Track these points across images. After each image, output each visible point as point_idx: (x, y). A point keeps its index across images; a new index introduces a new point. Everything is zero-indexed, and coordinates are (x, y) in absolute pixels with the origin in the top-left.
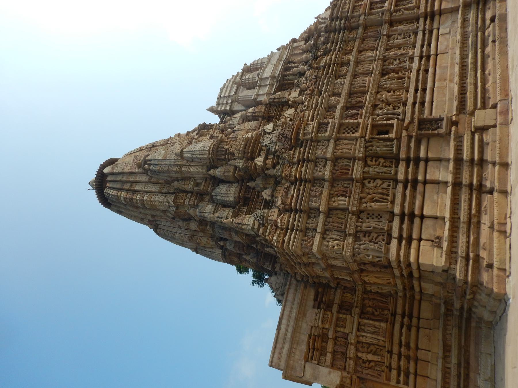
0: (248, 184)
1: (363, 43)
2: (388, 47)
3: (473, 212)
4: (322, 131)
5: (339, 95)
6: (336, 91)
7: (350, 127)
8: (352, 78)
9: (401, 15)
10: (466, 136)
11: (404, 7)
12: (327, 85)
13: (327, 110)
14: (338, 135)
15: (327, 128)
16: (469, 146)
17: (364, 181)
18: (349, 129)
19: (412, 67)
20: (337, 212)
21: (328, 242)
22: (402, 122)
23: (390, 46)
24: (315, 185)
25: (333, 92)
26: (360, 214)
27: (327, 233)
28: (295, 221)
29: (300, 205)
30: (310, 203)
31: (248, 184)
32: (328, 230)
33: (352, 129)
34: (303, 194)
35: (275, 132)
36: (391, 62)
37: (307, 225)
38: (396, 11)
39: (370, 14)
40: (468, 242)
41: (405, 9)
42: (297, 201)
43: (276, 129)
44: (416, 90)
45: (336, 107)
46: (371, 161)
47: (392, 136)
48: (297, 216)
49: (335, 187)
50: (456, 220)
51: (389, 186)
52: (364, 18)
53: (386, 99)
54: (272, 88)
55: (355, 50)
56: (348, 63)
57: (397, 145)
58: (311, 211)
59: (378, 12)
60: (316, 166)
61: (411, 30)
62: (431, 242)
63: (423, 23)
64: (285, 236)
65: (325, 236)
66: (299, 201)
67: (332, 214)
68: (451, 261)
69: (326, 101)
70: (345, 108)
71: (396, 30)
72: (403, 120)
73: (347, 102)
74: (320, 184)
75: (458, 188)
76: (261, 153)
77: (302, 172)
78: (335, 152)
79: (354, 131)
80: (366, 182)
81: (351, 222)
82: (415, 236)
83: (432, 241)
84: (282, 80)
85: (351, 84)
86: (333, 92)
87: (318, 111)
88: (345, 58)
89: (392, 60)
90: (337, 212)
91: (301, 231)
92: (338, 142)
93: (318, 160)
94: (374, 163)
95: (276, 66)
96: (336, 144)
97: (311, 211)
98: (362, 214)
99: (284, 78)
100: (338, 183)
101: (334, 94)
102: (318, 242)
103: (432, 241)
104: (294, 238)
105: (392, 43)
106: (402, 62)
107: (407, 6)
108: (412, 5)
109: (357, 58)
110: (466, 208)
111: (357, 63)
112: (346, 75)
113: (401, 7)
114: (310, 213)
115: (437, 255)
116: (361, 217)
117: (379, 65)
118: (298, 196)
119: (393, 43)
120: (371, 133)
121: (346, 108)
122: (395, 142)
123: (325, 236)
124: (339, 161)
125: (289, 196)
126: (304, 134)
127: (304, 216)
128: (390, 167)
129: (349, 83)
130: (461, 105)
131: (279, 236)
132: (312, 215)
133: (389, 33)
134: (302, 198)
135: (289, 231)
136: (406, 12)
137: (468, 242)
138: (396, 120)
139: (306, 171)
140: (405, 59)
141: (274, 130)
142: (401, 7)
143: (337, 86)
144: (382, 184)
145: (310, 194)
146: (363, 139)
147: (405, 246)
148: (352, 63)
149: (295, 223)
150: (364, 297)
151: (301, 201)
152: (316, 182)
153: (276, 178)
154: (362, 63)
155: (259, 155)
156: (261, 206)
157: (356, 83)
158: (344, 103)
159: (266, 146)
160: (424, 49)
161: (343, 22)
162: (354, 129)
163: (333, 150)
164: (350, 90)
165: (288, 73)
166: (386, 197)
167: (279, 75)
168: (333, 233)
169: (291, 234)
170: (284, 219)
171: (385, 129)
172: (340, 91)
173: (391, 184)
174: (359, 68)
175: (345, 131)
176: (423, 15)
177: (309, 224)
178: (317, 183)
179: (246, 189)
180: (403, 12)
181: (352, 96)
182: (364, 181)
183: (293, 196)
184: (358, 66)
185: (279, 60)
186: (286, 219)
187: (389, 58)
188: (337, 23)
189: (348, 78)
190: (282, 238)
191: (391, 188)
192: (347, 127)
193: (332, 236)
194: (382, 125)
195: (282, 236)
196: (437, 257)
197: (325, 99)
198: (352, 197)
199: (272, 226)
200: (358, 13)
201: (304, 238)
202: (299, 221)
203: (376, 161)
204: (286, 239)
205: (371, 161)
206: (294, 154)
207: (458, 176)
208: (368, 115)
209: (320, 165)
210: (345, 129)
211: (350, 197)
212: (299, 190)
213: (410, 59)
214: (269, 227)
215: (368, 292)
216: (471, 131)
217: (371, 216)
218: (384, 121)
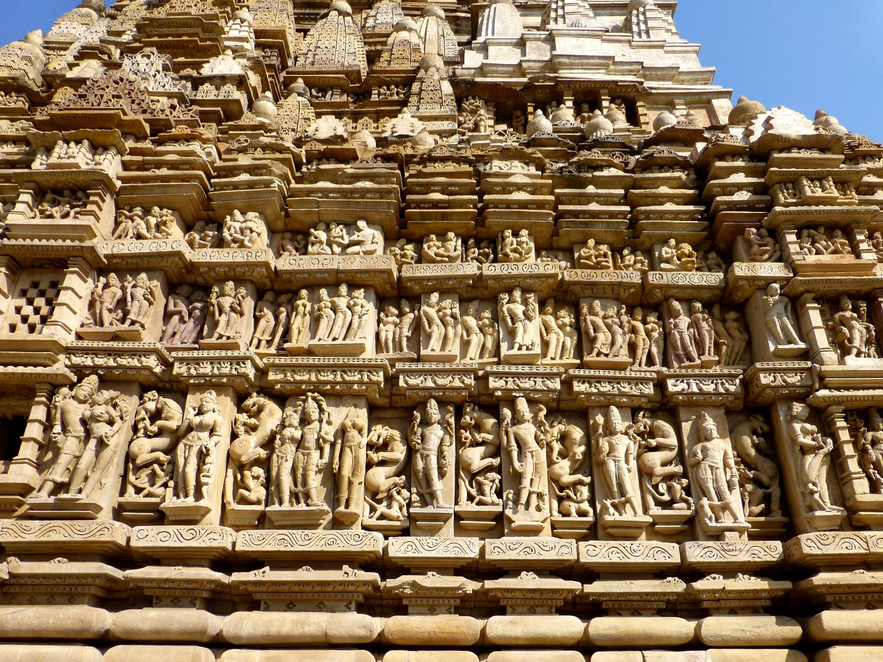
9: (793, 440)
11: (849, 450)
19: (433, 532)
38: (820, 416)
39: (795, 304)
41: (836, 461)
52: (775, 280)
53: (190, 429)
59: (805, 332)
61: (699, 510)
63: (743, 557)
71: (700, 435)
85: (334, 281)
106: (480, 486)
107: (853, 465)
108: (861, 487)
113: (844, 435)
129: (337, 271)
136: (815, 468)
140: (490, 496)
142: (844, 435)
143: (337, 230)
154: (487, 314)
157: (342, 302)
161: (743, 196)
176: (796, 556)
180: (814, 450)
187: (500, 419)
188: (739, 178)
200: (794, 248)
208: (100, 361)
213: (500, 518)
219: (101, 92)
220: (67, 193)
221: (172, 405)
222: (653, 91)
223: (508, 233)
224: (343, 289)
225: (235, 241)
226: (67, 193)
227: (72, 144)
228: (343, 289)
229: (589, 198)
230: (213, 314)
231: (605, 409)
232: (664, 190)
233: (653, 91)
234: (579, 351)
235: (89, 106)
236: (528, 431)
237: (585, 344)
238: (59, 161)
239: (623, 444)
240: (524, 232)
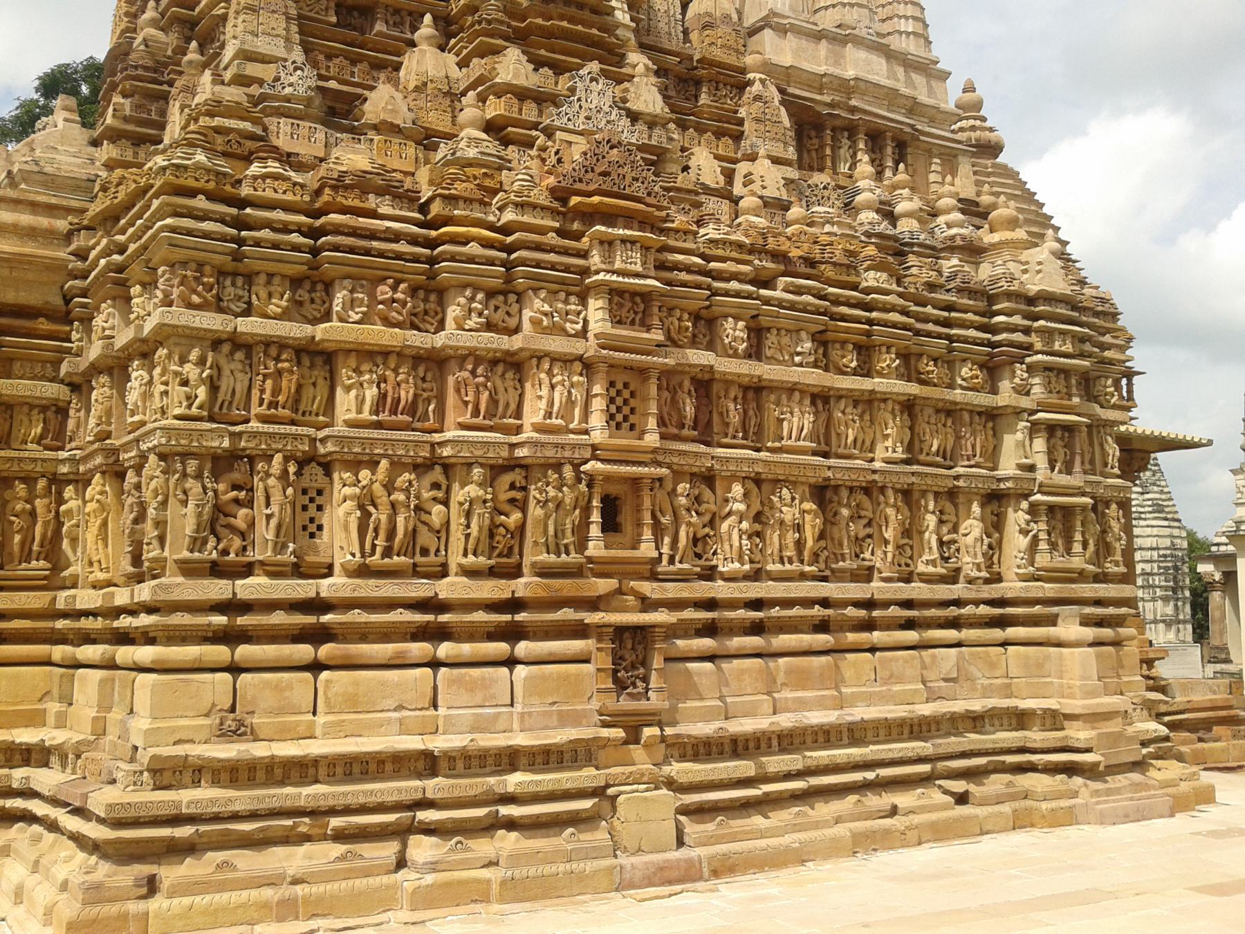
0: (428, 18)
1: (938, 411)
2: (916, 495)
3: (336, 822)
4: (621, 306)
5: (755, 352)
6: (772, 338)
7: (632, 402)
8: (816, 390)
10: (592, 771)
12: (792, 306)
13: (704, 313)
14: (603, 367)
15: (633, 323)
16: (556, 787)
17: (438, 468)
18: (626, 402)
20: (320, 382)
21: (201, 362)
22: (648, 575)
23: (918, 501)
24: (421, 294)
25: (768, 329)
26: (319, 464)
27: (239, 355)
28: (274, 230)
29: (336, 248)
30: (347, 282)
31: (428, 18)
32: (249, 356)
33: (626, 410)
34: (381, 254)
35: (625, 122)
36: (863, 513)
37: (262, 279)
40: (236, 817)
42: (354, 232)
43: (640, 126)
44: (757, 604)
45: (710, 347)
46: (512, 486)
47: (595, 548)
48: (295, 238)
49: (415, 368)
50: (312, 771)
51: (425, 552)
54: (810, 87)
55: (914, 389)
56: (865, 370)
57: (565, 565)
58: (319, 287)
60: (491, 294)
62: (228, 705)
63: (985, 595)
64: (211, 197)
65: (226, 348)
66: (350, 241)
67: (312, 367)
68: (167, 774)
69: (733, 311)
70: (707, 377)
72: (654, 577)
73: (728, 382)
74: (426, 312)
75: (421, 765)
76: (545, 71)
77: (466, 244)
78: (540, 358)
79: (619, 417)
80: (437, 474)
81: (285, 436)
82: (245, 651)
83: (233, 709)
84: (838, 123)
85: (791, 389)
86: (768, 329)
87: (698, 287)
88: (887, 361)
89: (871, 516)
90: (320, 382)
91: (237, 257)
92: (578, 366)
93: (512, 298)
94: (504, 496)
95: (891, 97)
96: (571, 361)
97: (319, 287)
98: (320, 471)
99: (844, 129)
100: (429, 376)
101: (757, 333)
102: (197, 324)
103: (233, 709)
104: (206, 235)
105: (926, 507)
109: (885, 401)
110: (351, 800)
111: (868, 403)
112: (826, 369)
114: (314, 283)
115: (183, 727)
116: (307, 470)
117: (853, 477)
118: (372, 235)
119: (927, 511)
120: (608, 478)
121: (704, 384)
122: (574, 558)
123: (226, 348)
124: (510, 375)
125: (372, 201)
126: (610, 243)
127: (297, 263)
128: (493, 548)
129: (796, 383)
130: (695, 746)
131: (208, 171)
132: (303, 294)
133: (964, 493)
134: (367, 252)
135: (234, 211)
137: (236, 817)
138: (655, 554)
139: (471, 260)
141: (634, 117)
144: (431, 529)
145: (383, 280)
146: (588, 455)
147: (209, 625)
148: (866, 384)
149: (265, 234)
150: (36, 480)
151: (352, 250)
152: (433, 297)
153: (450, 137)
154: (867, 417)
155: (538, 64)
156: (340, 82)
158: (725, 374)
159: (572, 90)
160: (894, 611)
162: (626, 418)
163: (547, 354)
164: (771, 389)
165: (861, 145)
166: (379, 550)
167: (853, 110)
168: (239, 375)
169: (223, 222)
170: (285, 186)
171: (626, 518)
172: (769, 353)
173: (432, 558)
174: (849, 410)
175: (620, 386)
177: (269, 283)
178: (426, 300)
179: (410, 14)
181: (751, 395)
182: (438, 468)
183: (374, 214)
184: (856, 403)
185: (914, 107)
186: (280, 196)
189: (814, 377)
190: (200, 184)
191: (419, 559)
192: (633, 394)
193: (226, 372)
194: (638, 509)
195: (212, 185)
196: (173, 730)
197: (741, 306)
198: (375, 434)
199: (253, 137)
201: (207, 269)
202: (276, 246)
203: (512, 501)
204: (201, 202)
205: (512, 486)
206: (534, 206)
207: (460, 765)
208: (675, 460)
209: (497, 308)
210: (626, 385)
211: (379, 425)
212: (396, 237)
214: (247, 126)
215: (60, 493)
216: (608, 786)
217: (312, 500)
218: (654, 516)
219: (620, 171)
220: (627, 295)
221: (707, 494)
222: (922, 138)
223: (884, 349)
224: (797, 394)
225: (731, 348)
226: (627, 295)
227: (629, 245)
228: (797, 395)
229: (926, 319)
230: (721, 414)
231: (924, 493)
232: (970, 316)
233: (922, 138)
234: (909, 448)
235: (615, 189)
236: (890, 511)
237: (917, 443)
238: (623, 266)
239: (931, 520)
240: (893, 350)
